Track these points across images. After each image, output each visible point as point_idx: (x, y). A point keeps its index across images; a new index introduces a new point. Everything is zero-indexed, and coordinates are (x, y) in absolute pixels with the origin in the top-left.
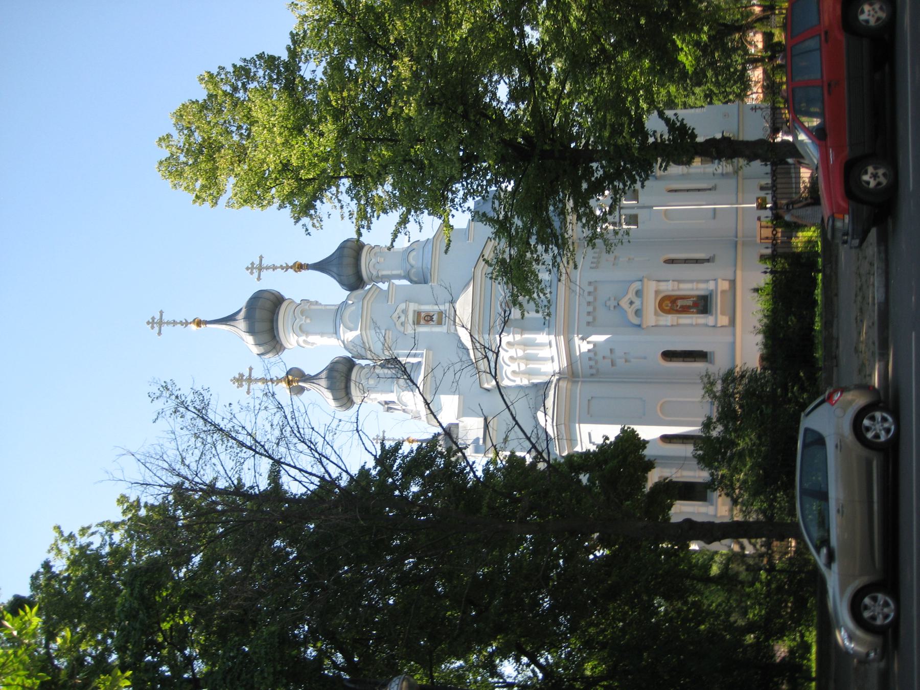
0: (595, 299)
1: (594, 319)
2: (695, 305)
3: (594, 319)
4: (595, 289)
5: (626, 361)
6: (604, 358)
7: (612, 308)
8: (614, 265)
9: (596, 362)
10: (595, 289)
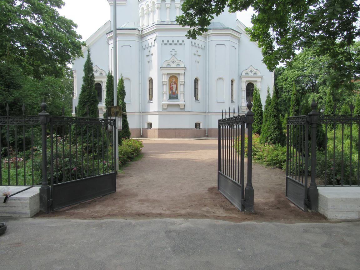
0: (176, 44)
1: (166, 44)
2: (174, 93)
3: (166, 44)
4: (181, 44)
5: (149, 62)
6: (149, 51)
7: (171, 53)
8: (194, 54)
9: (148, 48)
10: (181, 44)
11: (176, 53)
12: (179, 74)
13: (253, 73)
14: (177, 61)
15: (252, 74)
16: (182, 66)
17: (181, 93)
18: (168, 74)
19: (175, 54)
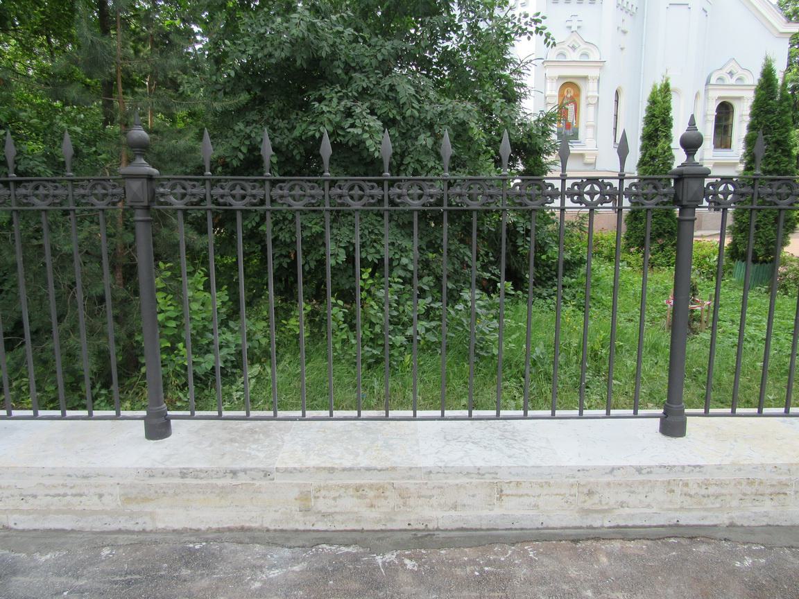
7: (569, 24)
11: (580, 24)
12: (585, 78)
13: (735, 77)
14: (583, 46)
15: (733, 81)
16: (594, 57)
17: (587, 127)
18: (560, 78)
19: (579, 27)
